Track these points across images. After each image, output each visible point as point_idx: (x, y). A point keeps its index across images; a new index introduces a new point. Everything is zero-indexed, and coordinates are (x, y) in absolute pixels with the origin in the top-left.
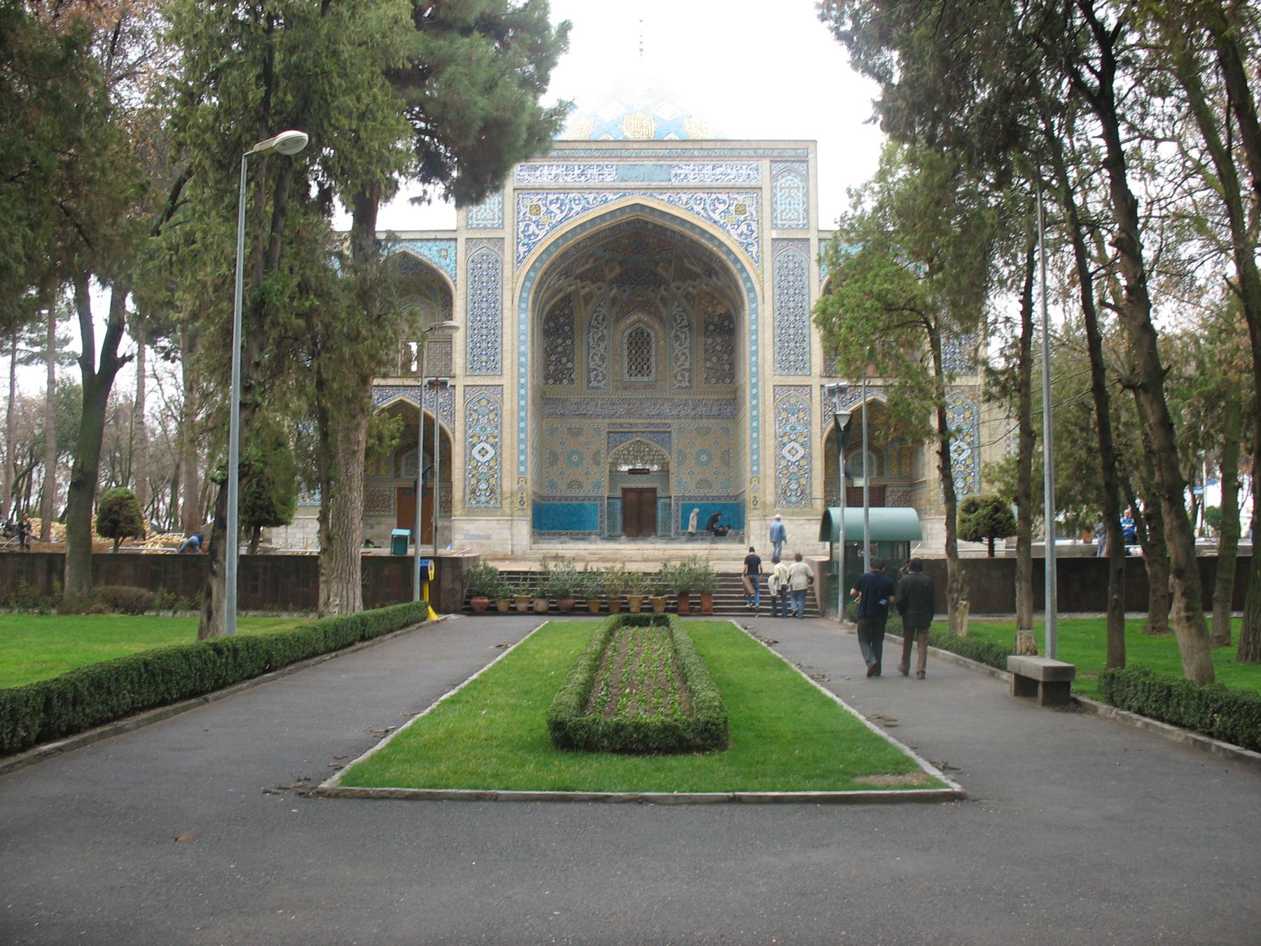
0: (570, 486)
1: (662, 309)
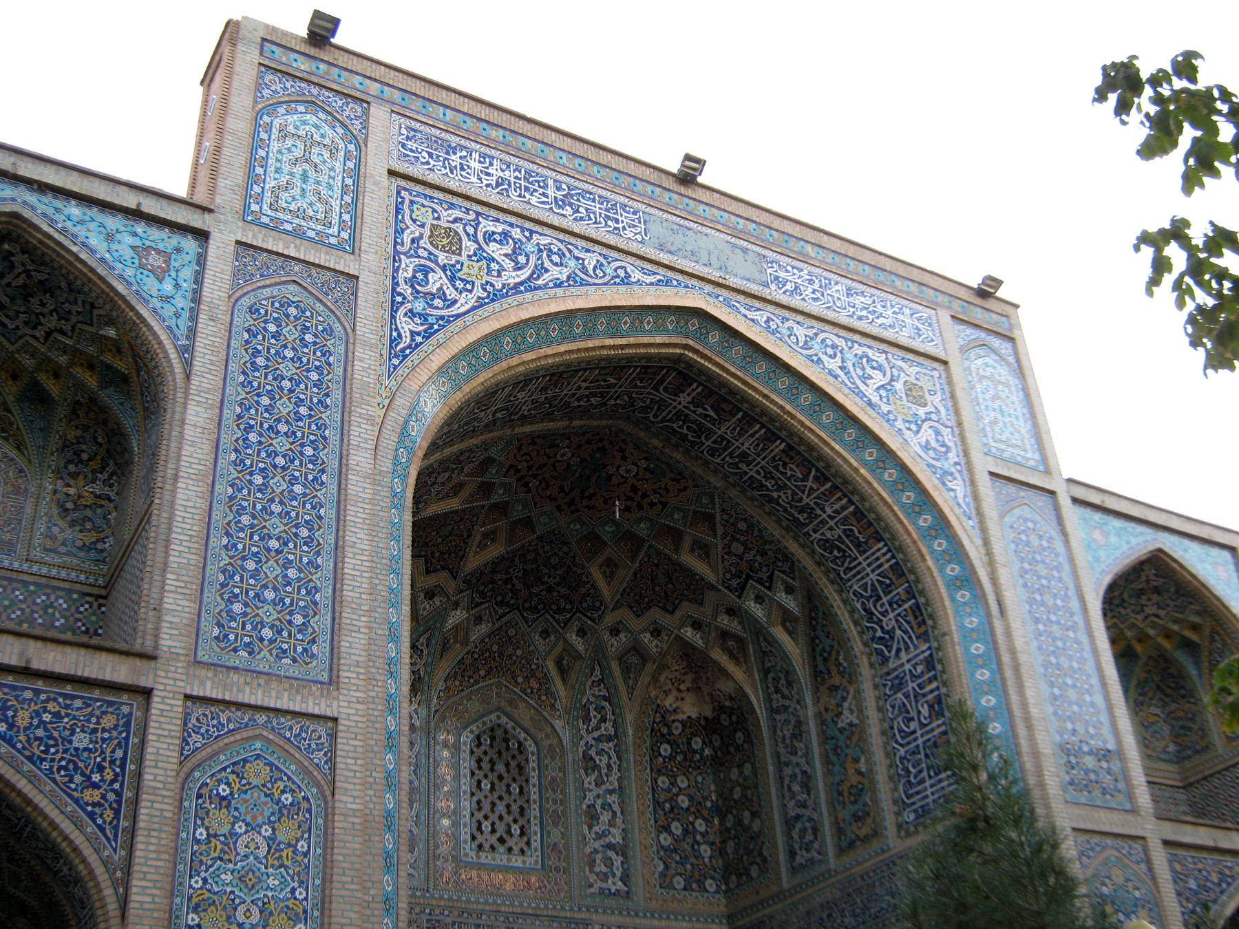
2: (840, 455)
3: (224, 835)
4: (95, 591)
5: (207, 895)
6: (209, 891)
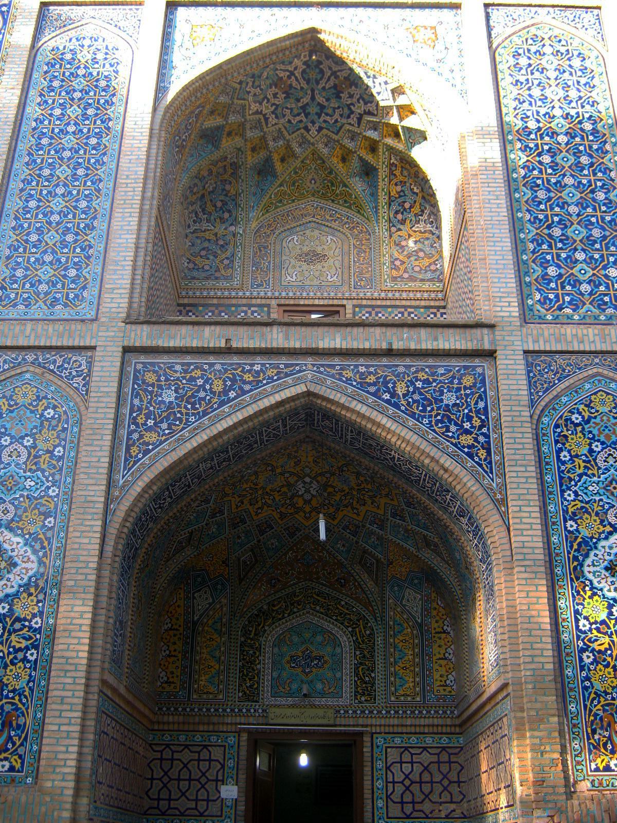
3: (585, 455)
4: (437, 304)
6: (581, 501)
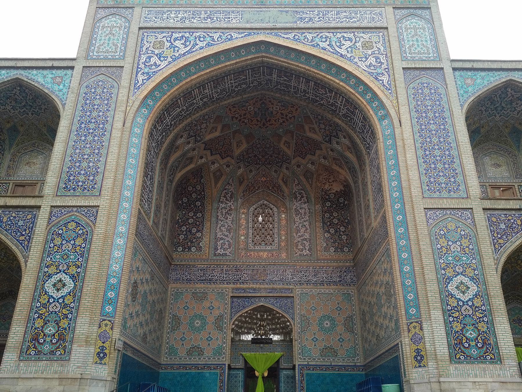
0: (189, 353)
1: (284, 187)
2: (332, 80)
5: (51, 262)
